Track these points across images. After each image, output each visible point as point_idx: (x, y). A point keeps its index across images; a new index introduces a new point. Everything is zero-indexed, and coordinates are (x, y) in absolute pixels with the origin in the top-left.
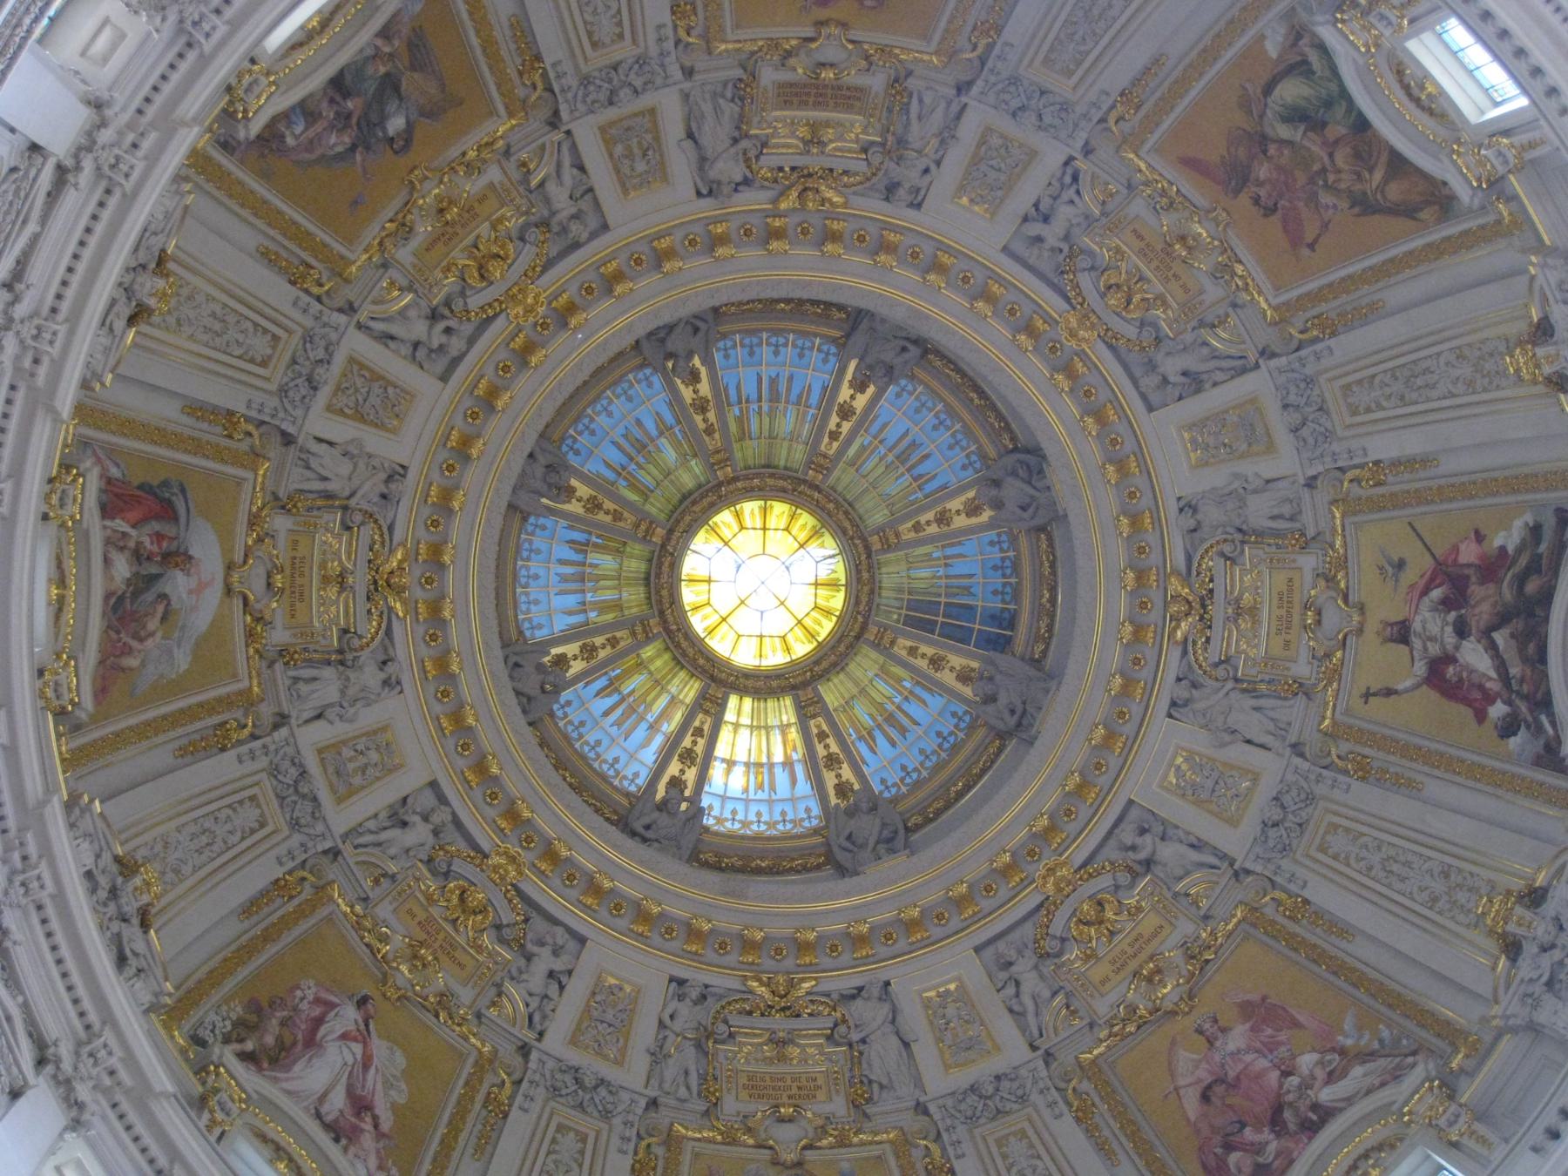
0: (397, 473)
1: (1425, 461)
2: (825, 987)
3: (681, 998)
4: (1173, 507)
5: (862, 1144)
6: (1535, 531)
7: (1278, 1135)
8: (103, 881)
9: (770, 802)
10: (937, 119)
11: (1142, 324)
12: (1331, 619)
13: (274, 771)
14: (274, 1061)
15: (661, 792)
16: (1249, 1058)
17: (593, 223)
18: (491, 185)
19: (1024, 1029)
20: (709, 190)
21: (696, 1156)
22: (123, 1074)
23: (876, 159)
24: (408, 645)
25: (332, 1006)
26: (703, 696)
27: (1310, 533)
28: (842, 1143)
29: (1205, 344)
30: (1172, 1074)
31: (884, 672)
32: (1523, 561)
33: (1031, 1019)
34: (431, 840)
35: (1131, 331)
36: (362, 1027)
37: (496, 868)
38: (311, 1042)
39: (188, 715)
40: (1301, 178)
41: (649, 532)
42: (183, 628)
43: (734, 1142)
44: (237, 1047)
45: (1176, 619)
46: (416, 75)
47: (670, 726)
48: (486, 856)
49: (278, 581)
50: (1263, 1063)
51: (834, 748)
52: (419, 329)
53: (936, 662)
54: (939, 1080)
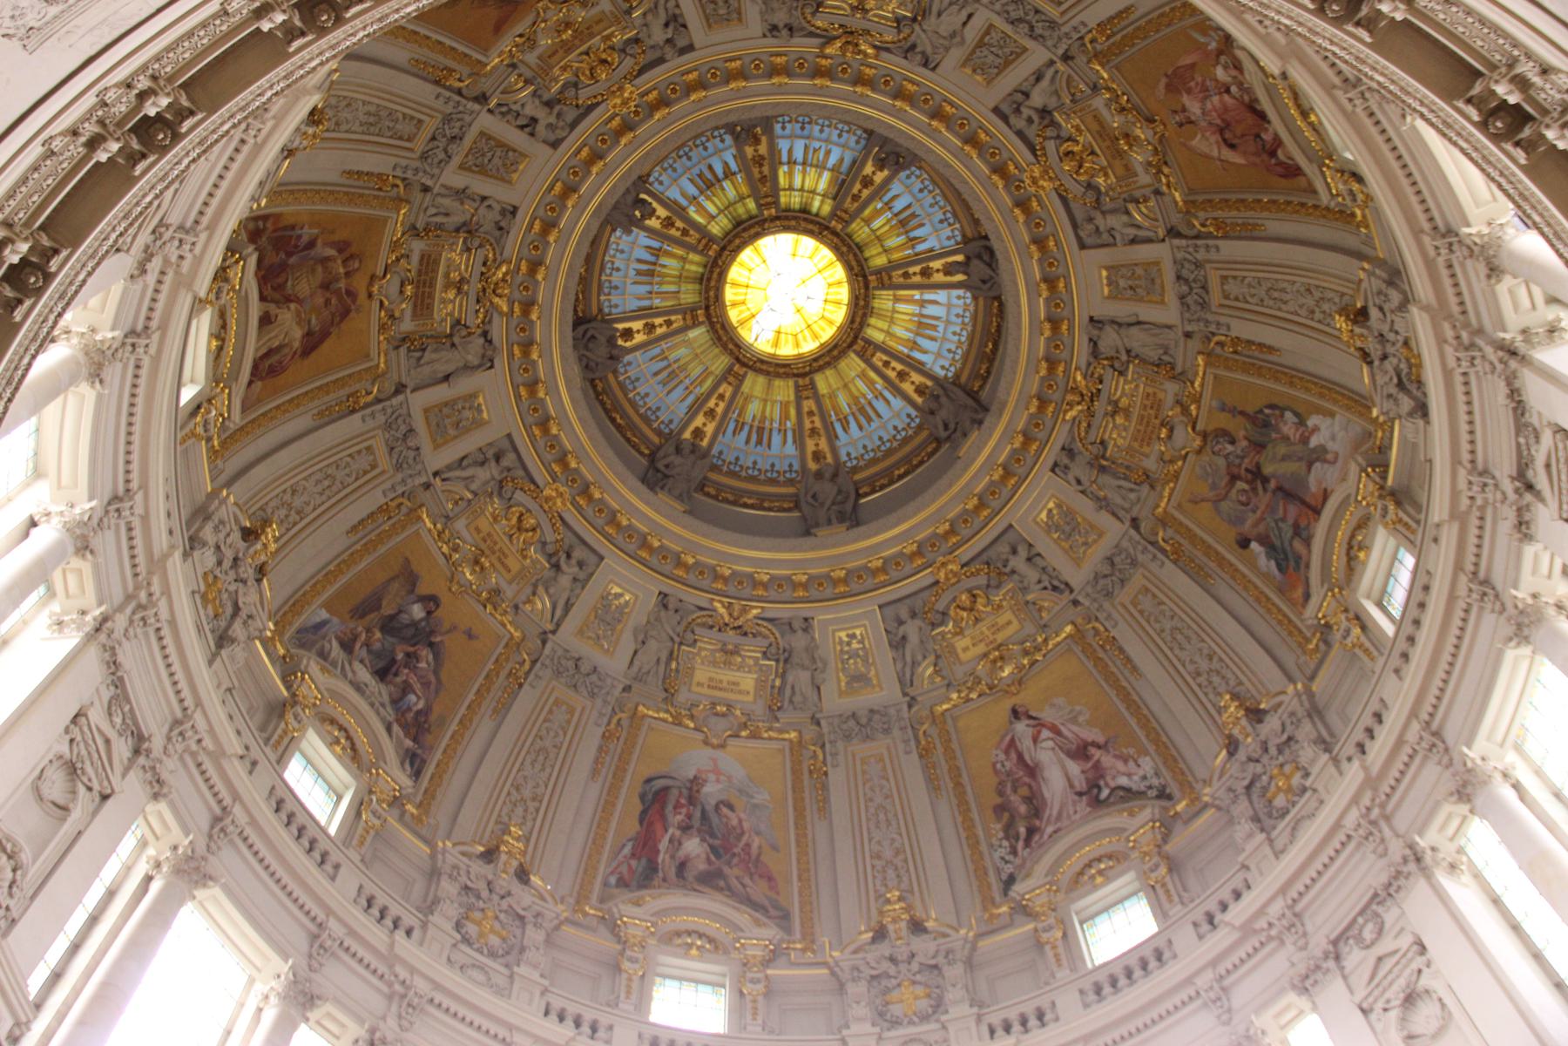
2: (1083, 366)
4: (770, 41)
5: (1202, 385)
9: (948, 322)
10: (446, 202)
13: (848, 737)
16: (1209, 106)
20: (488, 363)
21: (1179, 507)
23: (476, 243)
25: (1012, 741)
28: (1197, 400)
30: (1207, 156)
34: (918, 622)
35: (629, 62)
36: (1032, 722)
37: (947, 579)
38: (1032, 771)
41: (736, 376)
42: (740, 791)
43: (1176, 476)
46: (384, 603)
48: (937, 582)
50: (1216, 99)
52: (565, 581)
54: (1169, 313)
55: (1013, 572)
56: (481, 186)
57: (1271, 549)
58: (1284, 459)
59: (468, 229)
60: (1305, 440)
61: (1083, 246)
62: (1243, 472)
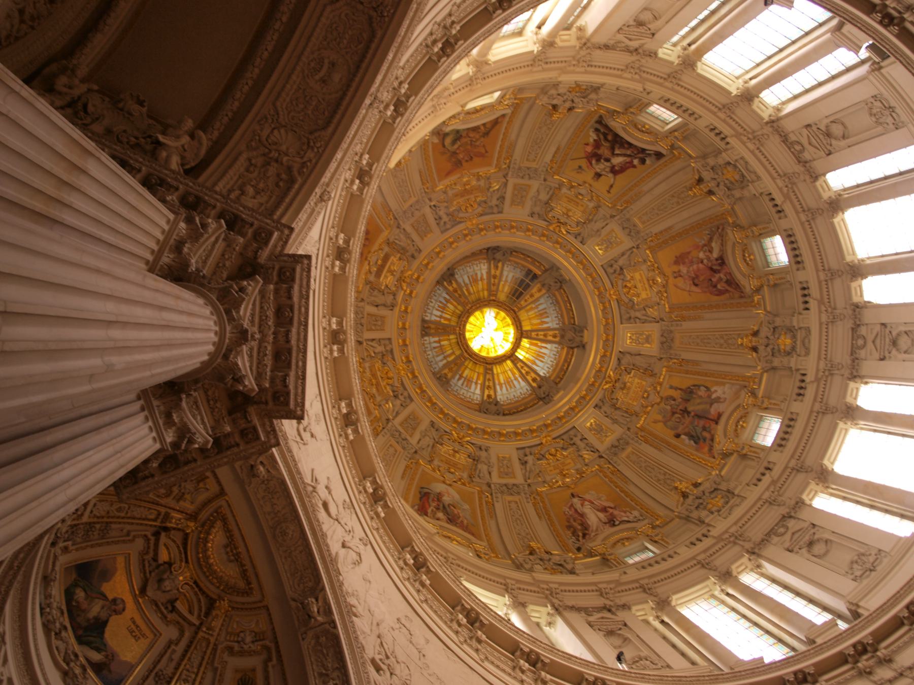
0: (432, 424)
1: (558, 149)
3: (600, 408)
4: (530, 218)
5: (664, 379)
6: (597, 130)
7: (719, 272)
8: (538, 561)
10: (402, 236)
11: (479, 205)
12: (582, 190)
14: (586, 529)
15: (534, 385)
17: (387, 342)
18: (369, 367)
19: (651, 322)
20: (392, 307)
22: (612, 586)
24: (478, 441)
26: (513, 362)
27: (557, 186)
28: (661, 384)
29: (494, 191)
30: (684, 290)
31: (528, 311)
32: (602, 137)
33: (650, 319)
34: (532, 457)
37: (546, 442)
38: (582, 515)
39: (482, 511)
40: (469, 147)
43: (648, 413)
44: (580, 538)
45: (560, 231)
47: (517, 375)
49: (452, 470)
50: (695, 267)
51: (542, 333)
52: (398, 402)
53: (532, 296)
55: (574, 444)
56: (415, 236)
57: (691, 437)
58: (699, 404)
59: (403, 251)
60: (709, 396)
61: (622, 323)
62: (678, 411)
